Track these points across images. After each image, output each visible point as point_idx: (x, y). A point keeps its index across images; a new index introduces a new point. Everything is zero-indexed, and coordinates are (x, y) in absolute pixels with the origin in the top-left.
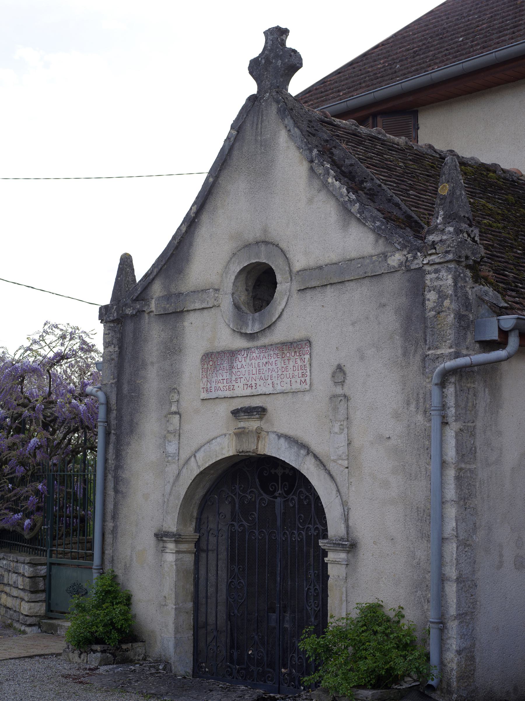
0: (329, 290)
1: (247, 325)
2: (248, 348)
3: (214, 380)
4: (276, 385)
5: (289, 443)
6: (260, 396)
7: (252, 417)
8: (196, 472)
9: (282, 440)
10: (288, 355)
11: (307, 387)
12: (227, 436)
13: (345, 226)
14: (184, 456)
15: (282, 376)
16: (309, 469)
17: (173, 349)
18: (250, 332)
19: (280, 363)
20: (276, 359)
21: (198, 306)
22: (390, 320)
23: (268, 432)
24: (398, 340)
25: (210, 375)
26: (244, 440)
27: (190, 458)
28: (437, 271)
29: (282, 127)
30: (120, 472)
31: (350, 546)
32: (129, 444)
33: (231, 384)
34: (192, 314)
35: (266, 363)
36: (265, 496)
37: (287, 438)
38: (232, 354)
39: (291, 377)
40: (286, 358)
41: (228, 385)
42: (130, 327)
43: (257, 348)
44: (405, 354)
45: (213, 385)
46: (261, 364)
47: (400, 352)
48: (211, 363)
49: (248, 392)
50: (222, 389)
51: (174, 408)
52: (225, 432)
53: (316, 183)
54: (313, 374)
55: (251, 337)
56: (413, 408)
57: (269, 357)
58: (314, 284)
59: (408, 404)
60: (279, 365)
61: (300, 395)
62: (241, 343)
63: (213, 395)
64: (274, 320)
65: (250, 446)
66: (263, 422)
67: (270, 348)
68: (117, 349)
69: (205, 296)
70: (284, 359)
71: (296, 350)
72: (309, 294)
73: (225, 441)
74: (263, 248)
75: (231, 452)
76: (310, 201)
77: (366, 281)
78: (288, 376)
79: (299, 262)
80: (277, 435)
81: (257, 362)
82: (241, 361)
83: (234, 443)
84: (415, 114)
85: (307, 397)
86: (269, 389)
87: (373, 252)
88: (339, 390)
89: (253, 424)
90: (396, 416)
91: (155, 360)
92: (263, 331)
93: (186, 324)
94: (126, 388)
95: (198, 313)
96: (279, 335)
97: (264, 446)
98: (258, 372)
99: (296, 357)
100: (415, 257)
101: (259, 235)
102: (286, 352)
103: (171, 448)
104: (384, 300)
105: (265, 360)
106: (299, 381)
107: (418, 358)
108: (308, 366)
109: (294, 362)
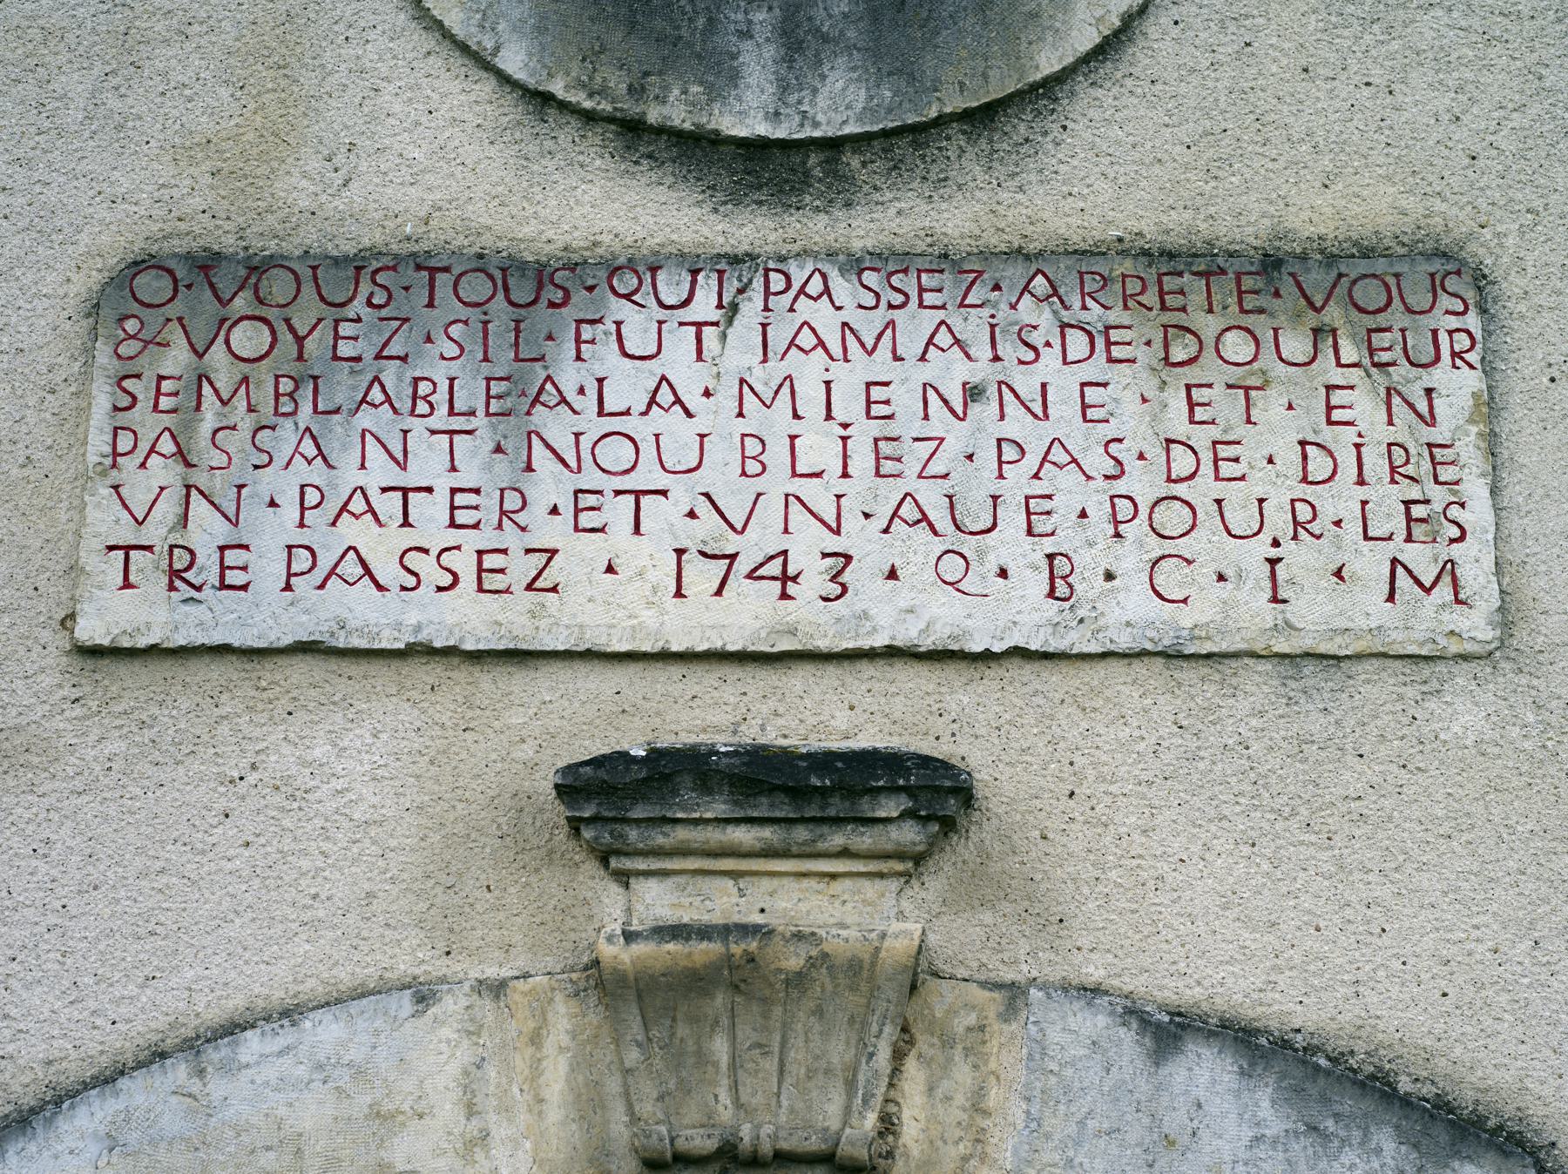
1: (721, 75)
2: (735, 260)
3: (284, 483)
4: (1088, 585)
5: (1292, 1095)
6: (867, 669)
7: (837, 840)
9: (1204, 1071)
10: (1237, 347)
11: (1477, 625)
12: (451, 1005)
15: (1173, 518)
18: (763, 129)
19: (1137, 404)
20: (1089, 372)
23: (1014, 994)
25: (236, 442)
26: (720, 1047)
33: (510, 537)
35: (973, 393)
37: (1253, 1044)
38: (537, 293)
39: (1278, 521)
40: (1208, 369)
41: (471, 541)
43: (855, 266)
45: (271, 533)
46: (904, 399)
48: (249, 339)
49: (747, 616)
50: (388, 571)
52: (410, 957)
54: (1514, 524)
57: (1009, 349)
60: (1131, 421)
61: (1377, 689)
63: (264, 618)
64: (1048, 62)
66: (934, 886)
67: (1014, 273)
70: (1192, 374)
71: (1334, 314)
78: (1242, 519)
80: (1134, 1013)
81: (849, 381)
82: (617, 363)
83: (557, 1075)
85: (1464, 711)
86: (1023, 614)
89: (831, 906)
92: (904, 144)
97: (978, 1107)
98: (862, 461)
99: (1337, 376)
102: (1208, 325)
105: (952, 372)
106: (1370, 564)
108: (1469, 449)
109: (1289, 413)
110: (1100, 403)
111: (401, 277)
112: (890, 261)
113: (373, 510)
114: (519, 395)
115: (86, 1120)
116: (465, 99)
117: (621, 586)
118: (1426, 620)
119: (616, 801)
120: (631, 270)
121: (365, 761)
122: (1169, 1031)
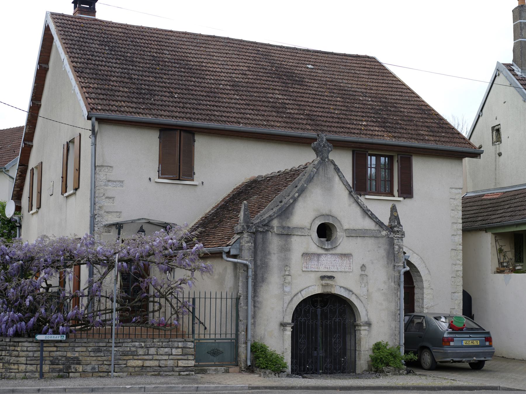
0: (359, 239)
1: (325, 245)
8: (302, 299)
9: (342, 289)
13: (364, 218)
14: (294, 292)
16: (353, 299)
17: (286, 249)
21: (299, 234)
22: (382, 252)
24: (385, 259)
27: (298, 293)
28: (398, 240)
29: (336, 175)
30: (256, 298)
31: (369, 324)
32: (261, 286)
34: (295, 236)
36: (313, 308)
37: (344, 288)
38: (319, 255)
42: (260, 237)
44: (388, 263)
45: (310, 266)
47: (386, 263)
49: (326, 270)
51: (287, 273)
53: (352, 200)
55: (327, 250)
56: (390, 281)
58: (353, 235)
59: (389, 279)
62: (322, 252)
65: (328, 290)
68: (253, 245)
69: (303, 230)
72: (351, 238)
73: (316, 288)
74: (331, 218)
75: (319, 292)
76: (350, 205)
77: (373, 238)
79: (346, 227)
84: (193, 135)
85: (351, 274)
86: (336, 270)
87: (375, 229)
88: (363, 273)
89: (329, 282)
90: (385, 282)
91: (276, 252)
93: (292, 240)
94: (259, 262)
95: (298, 237)
96: (339, 250)
100: (390, 234)
101: (328, 212)
103: (287, 289)
104: (380, 246)
107: (392, 265)
109: (346, 261)
110: (338, 260)
111: (314, 254)
112: (332, 254)
113: (313, 265)
114: (318, 260)
115: (304, 290)
116: (315, 246)
117: (322, 269)
118: (350, 270)
119: (323, 278)
120: (322, 254)
121: (313, 276)
122: (341, 287)
